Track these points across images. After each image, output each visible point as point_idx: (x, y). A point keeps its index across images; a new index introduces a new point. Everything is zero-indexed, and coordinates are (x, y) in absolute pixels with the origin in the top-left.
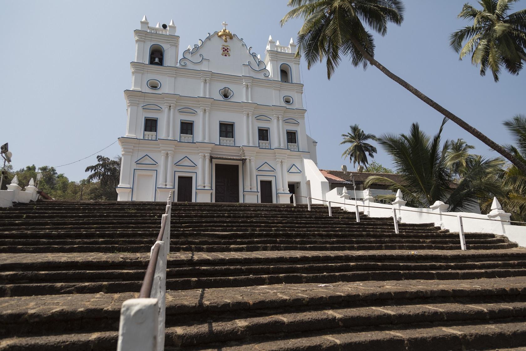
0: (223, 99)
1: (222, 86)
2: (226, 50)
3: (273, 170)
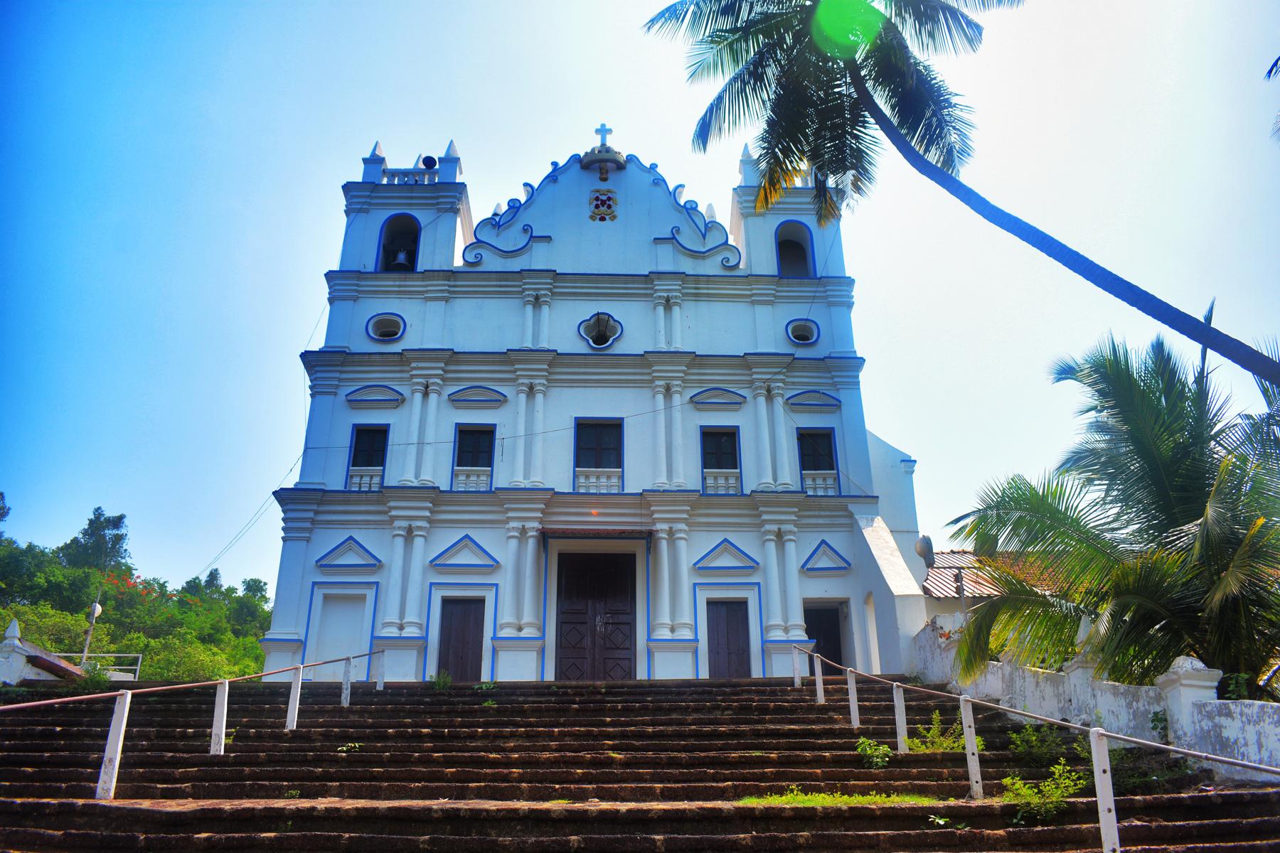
0: (585, 350)
1: (587, 310)
2: (603, 203)
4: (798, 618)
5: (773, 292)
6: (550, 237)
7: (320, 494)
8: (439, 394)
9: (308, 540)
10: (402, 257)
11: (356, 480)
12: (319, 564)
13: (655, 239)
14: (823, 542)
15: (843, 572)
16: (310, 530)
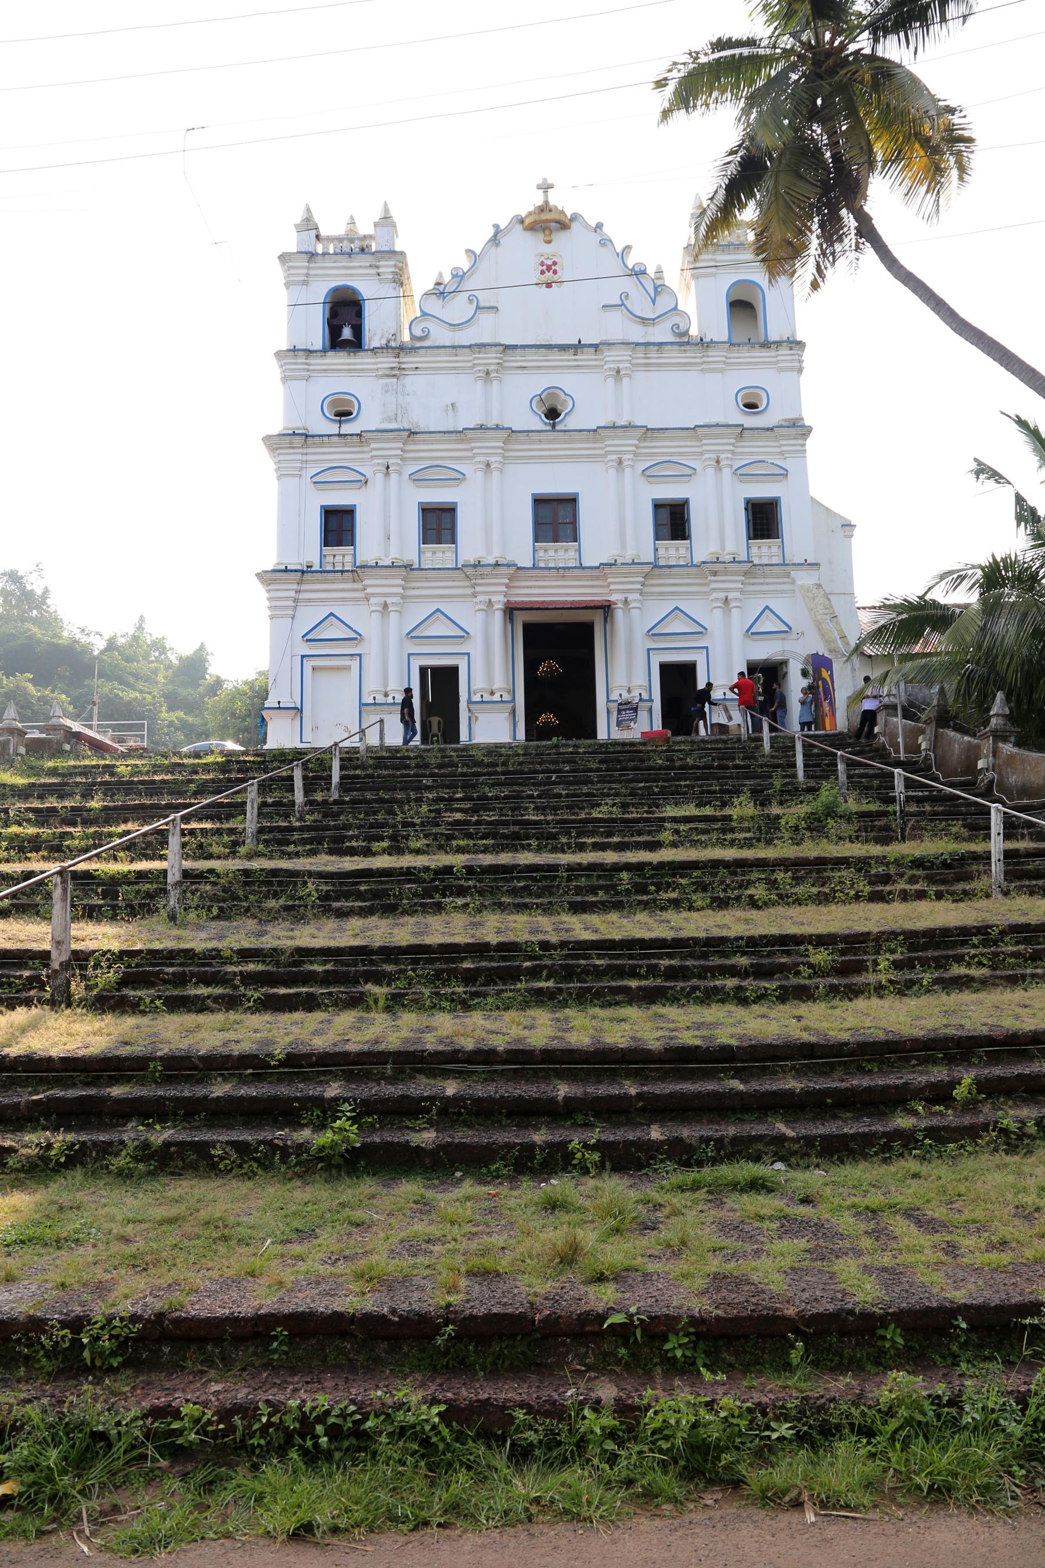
0: (540, 426)
1: (537, 383)
2: (549, 268)
3: (701, 630)
6: (496, 308)
7: (299, 574)
8: (400, 473)
11: (330, 559)
14: (767, 607)
15: (783, 635)
16: (295, 607)
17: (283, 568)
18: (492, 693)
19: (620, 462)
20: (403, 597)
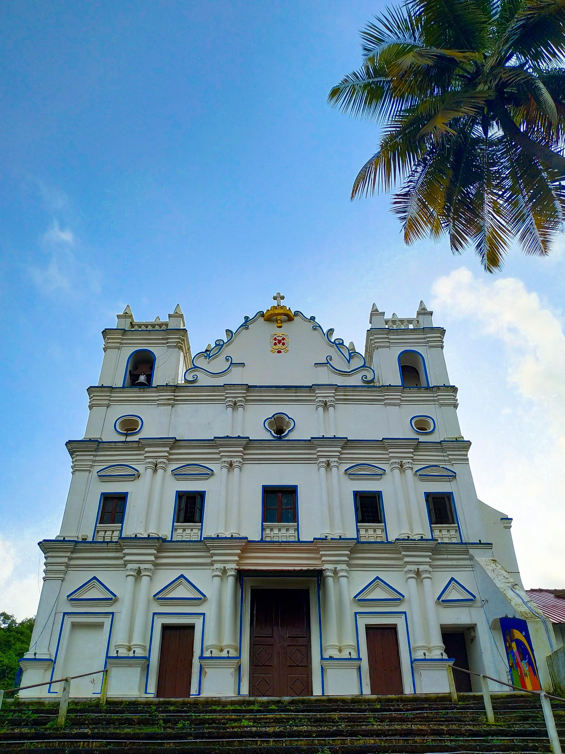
2: (279, 342)
3: (400, 597)
4: (437, 641)
5: (400, 397)
6: (244, 364)
8: (165, 469)
9: (63, 580)
10: (142, 378)
11: (101, 534)
12: (69, 598)
13: (315, 364)
14: (452, 579)
15: (470, 603)
16: (65, 573)
17: (62, 539)
18: (221, 650)
19: (328, 464)
20: (155, 565)
